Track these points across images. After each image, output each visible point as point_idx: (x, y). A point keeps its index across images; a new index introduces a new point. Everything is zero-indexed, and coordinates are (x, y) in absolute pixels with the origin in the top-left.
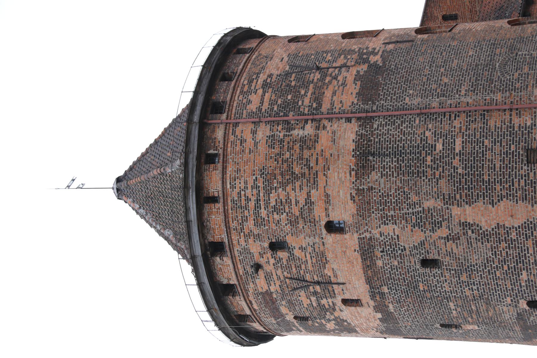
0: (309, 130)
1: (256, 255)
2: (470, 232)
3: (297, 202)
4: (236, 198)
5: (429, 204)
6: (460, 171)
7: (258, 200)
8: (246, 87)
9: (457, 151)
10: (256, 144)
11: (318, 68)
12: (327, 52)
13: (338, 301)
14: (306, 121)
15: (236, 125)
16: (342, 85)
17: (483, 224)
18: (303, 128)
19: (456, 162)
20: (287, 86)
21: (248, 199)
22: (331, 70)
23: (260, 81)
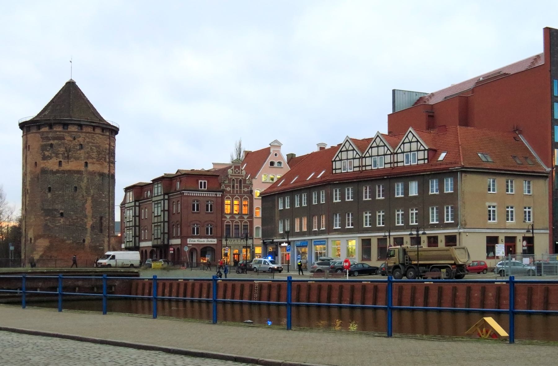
0: (108, 160)
13: (61, 160)
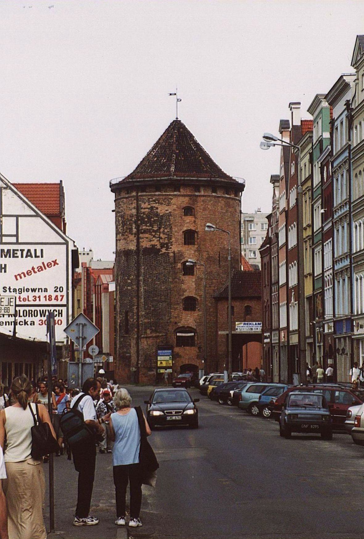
0: (134, 230)
11: (160, 228)
23: (154, 205)
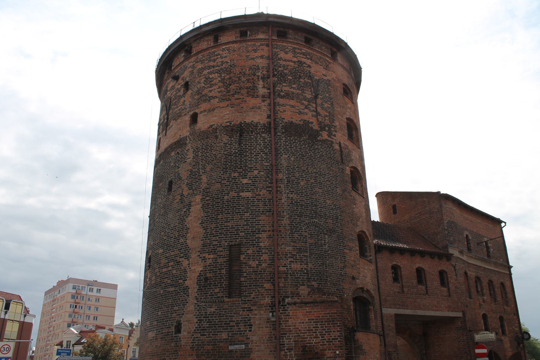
0: (262, 91)
1: (183, 76)
2: (185, 210)
3: (210, 91)
4: (216, 53)
5: (204, 178)
6: (226, 197)
7: (214, 67)
8: (300, 51)
9: (241, 194)
10: (253, 59)
11: (316, 97)
12: (332, 104)
14: (269, 89)
15: (267, 45)
16: (300, 112)
17: (189, 218)
18: (264, 87)
19: (233, 194)
20: (300, 76)
21: (214, 61)
22: (314, 105)
23: (304, 60)
